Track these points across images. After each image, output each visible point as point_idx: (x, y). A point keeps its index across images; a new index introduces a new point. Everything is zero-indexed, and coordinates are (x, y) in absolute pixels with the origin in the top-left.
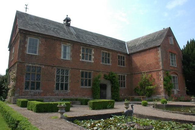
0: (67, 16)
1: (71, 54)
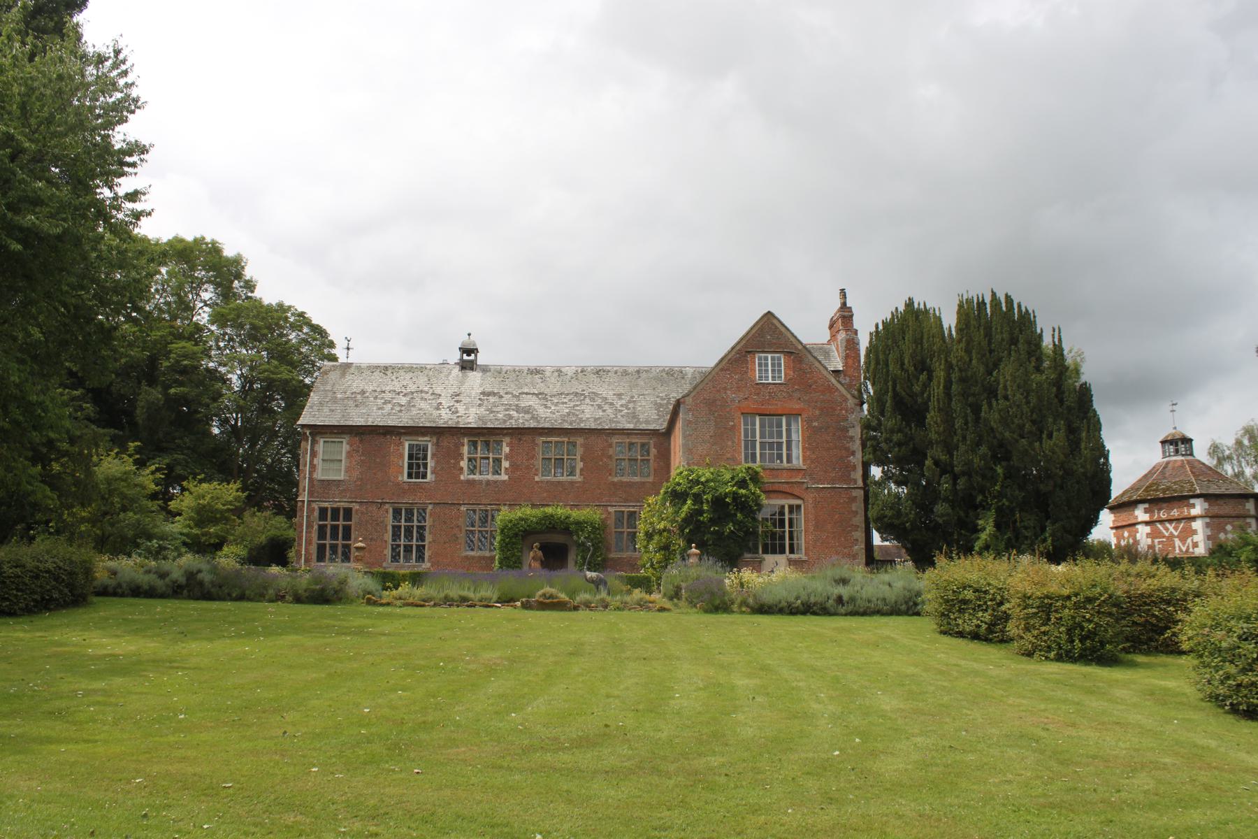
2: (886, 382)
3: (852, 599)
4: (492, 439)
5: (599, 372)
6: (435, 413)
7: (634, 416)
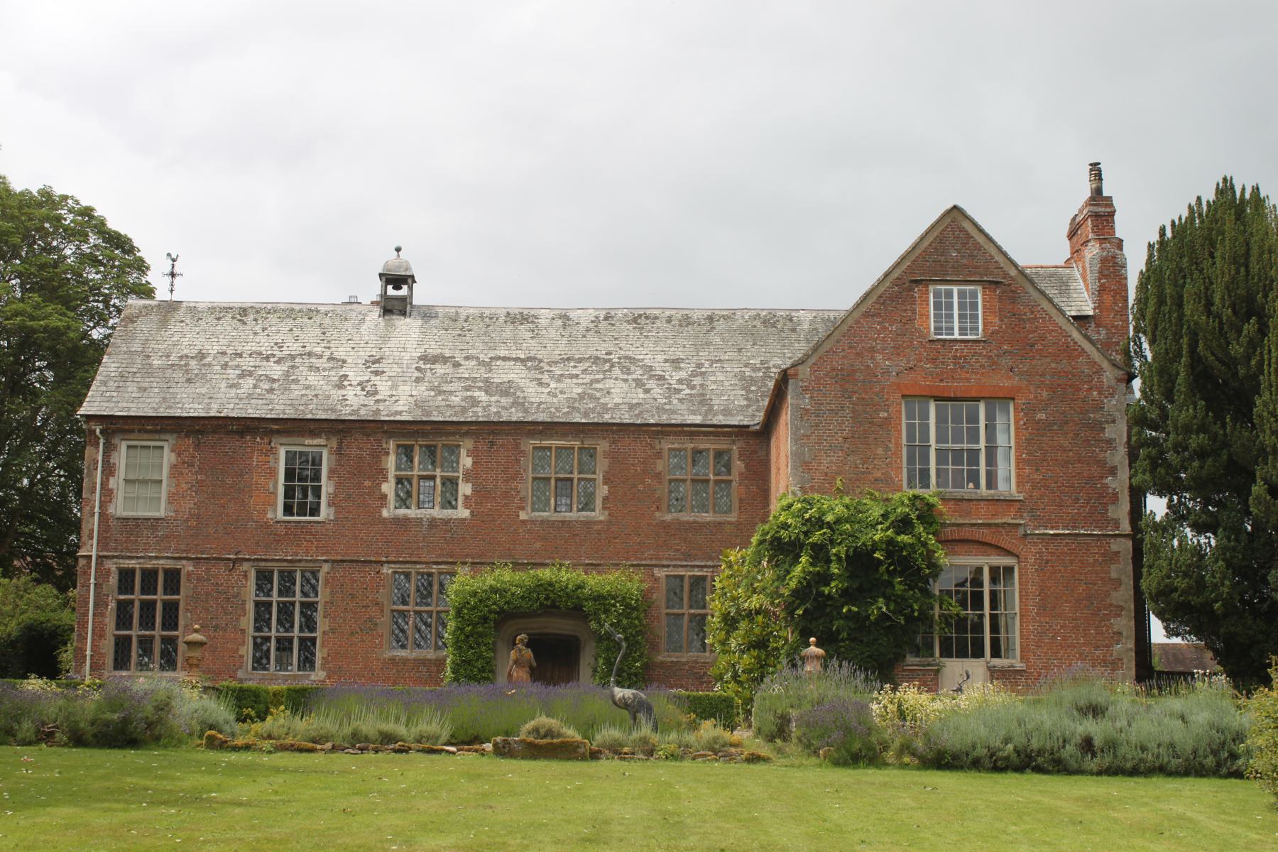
0: (398, 250)
1: (331, 490)
2: (1177, 337)
3: (1112, 745)
4: (440, 442)
5: (639, 319)
6: (336, 394)
7: (703, 400)
